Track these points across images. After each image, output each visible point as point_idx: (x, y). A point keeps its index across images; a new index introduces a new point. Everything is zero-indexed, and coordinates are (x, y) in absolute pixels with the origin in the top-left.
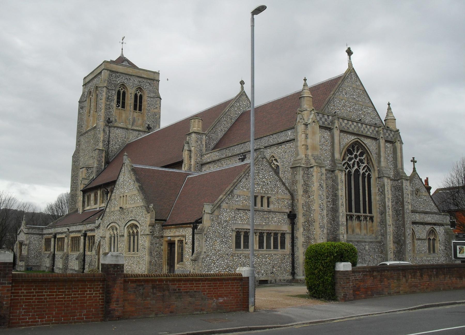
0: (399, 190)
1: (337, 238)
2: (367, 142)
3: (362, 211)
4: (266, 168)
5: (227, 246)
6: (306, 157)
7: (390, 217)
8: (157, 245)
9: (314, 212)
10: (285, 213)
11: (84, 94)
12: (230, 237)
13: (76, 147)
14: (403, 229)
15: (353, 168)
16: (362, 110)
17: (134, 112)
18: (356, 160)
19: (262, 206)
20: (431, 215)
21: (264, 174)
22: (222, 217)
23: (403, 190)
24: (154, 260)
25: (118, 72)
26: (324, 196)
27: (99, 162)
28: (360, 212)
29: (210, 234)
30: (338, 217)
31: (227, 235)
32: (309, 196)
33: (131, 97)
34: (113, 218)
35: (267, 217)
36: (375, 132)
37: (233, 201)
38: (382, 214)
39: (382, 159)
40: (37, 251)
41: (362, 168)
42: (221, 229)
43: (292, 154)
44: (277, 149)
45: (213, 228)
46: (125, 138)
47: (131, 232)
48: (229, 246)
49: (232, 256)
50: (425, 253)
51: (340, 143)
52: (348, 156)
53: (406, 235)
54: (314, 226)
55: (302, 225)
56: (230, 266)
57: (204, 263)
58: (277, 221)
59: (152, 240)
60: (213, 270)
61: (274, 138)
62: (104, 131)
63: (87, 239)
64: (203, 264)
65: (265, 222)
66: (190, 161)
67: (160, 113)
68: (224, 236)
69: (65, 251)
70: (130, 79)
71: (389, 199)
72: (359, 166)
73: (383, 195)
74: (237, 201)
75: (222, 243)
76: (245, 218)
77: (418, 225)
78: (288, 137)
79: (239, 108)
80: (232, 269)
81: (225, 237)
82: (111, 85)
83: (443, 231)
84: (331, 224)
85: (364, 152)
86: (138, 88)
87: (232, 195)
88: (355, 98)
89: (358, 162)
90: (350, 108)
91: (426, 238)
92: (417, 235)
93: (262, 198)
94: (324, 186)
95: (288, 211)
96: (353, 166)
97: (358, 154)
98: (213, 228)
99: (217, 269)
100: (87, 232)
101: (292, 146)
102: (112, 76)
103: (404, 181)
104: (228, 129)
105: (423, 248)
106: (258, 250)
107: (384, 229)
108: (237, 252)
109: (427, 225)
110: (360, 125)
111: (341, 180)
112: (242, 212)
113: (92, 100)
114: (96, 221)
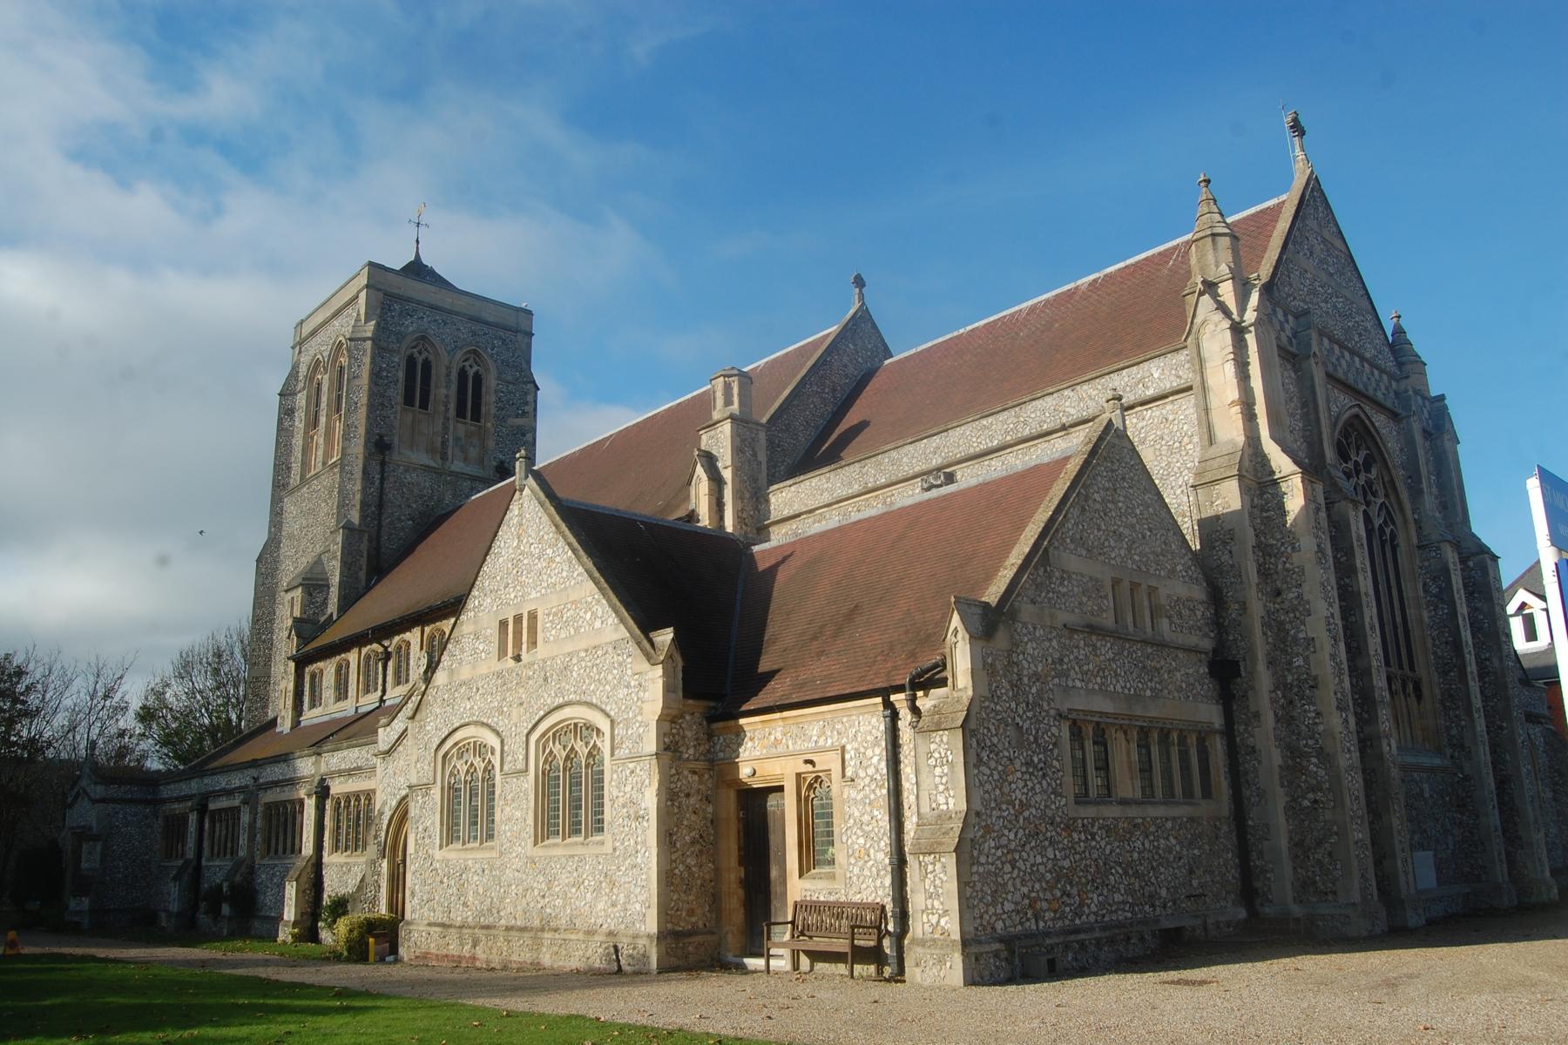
5: (1049, 784)
6: (1249, 445)
8: (692, 800)
9: (1307, 648)
13: (270, 532)
22: (1021, 657)
25: (409, 300)
29: (989, 730)
34: (466, 708)
35: (1155, 668)
37: (1051, 595)
42: (1024, 712)
43: (1177, 444)
46: (431, 498)
47: (560, 753)
49: (1067, 827)
54: (1314, 704)
61: (1081, 399)
63: (329, 805)
64: (975, 869)
67: (534, 430)
68: (1036, 738)
69: (241, 854)
71: (1464, 618)
78: (1148, 388)
81: (1039, 745)
86: (469, 352)
98: (998, 708)
100: (330, 782)
101: (1171, 418)
102: (390, 310)
106: (1143, 803)
107: (1463, 723)
111: (1359, 536)
113: (325, 388)
114: (381, 730)
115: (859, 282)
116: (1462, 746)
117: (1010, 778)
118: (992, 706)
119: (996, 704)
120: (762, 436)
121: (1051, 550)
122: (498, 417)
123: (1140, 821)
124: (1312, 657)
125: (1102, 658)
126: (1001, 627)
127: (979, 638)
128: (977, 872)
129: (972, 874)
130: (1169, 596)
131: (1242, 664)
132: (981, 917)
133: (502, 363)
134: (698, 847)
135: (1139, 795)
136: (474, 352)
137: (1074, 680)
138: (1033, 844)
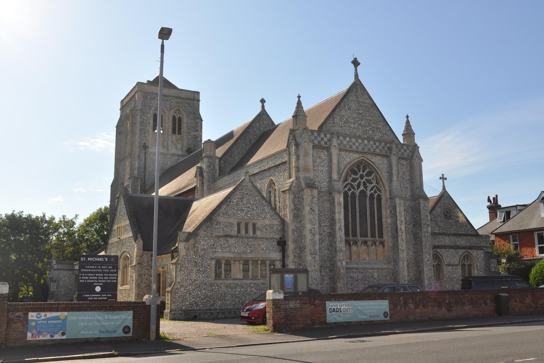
0: (416, 212)
1: (335, 265)
2: (376, 160)
3: (369, 235)
4: (251, 193)
5: (205, 275)
6: (297, 179)
7: (403, 241)
8: (146, 276)
10: (275, 240)
11: (122, 119)
12: (208, 266)
14: (421, 254)
15: (358, 189)
16: (369, 125)
17: (173, 135)
18: (361, 180)
19: (247, 231)
20: (465, 238)
21: (249, 199)
22: (199, 245)
23: (420, 212)
24: (142, 293)
26: (316, 220)
27: (134, 191)
28: (367, 237)
29: (185, 263)
30: (336, 242)
31: (205, 264)
32: (301, 221)
33: (168, 119)
35: (252, 244)
36: (386, 149)
37: (212, 229)
38: (394, 239)
39: (395, 178)
40: (67, 288)
41: (369, 189)
42: (198, 258)
44: (274, 171)
45: (189, 257)
46: (163, 164)
48: (207, 275)
50: (457, 280)
51: (338, 162)
52: (351, 176)
53: (424, 260)
55: (292, 251)
56: (208, 297)
57: (178, 293)
58: (265, 248)
59: (139, 272)
60: (188, 301)
62: (139, 157)
64: (177, 295)
65: (250, 250)
66: (203, 188)
67: (201, 136)
68: (202, 265)
70: (167, 101)
71: (402, 221)
72: (366, 187)
73: (395, 218)
74: (217, 228)
75: (199, 272)
76: (225, 246)
77: (447, 249)
79: (259, 129)
80: (211, 299)
81: (203, 266)
82: (146, 108)
83: (483, 255)
84: (328, 250)
85: (373, 171)
87: (211, 223)
88: (361, 113)
89: (364, 182)
90: (354, 124)
91: (459, 264)
92: (446, 261)
93: (247, 225)
94: (316, 209)
95: (278, 237)
96: (359, 186)
97: (364, 174)
98: (189, 257)
99: (194, 300)
102: (146, 98)
103: (421, 200)
104: (246, 152)
105: (455, 275)
106: (242, 279)
108: (217, 282)
109: (460, 249)
110: (366, 142)
112: (223, 240)
115: (263, 101)
116: (396, 261)
117: (191, 274)
118: (187, 257)
119: (188, 257)
120: (217, 161)
121: (213, 217)
122: (187, 132)
123: (240, 284)
124: (305, 240)
125: (230, 243)
126: (192, 238)
127: (184, 241)
128: (177, 295)
129: (175, 296)
130: (262, 224)
131: (287, 242)
132: (178, 305)
133: (189, 112)
134: (147, 288)
135: (242, 277)
136: (178, 109)
137: (218, 250)
138: (198, 289)
